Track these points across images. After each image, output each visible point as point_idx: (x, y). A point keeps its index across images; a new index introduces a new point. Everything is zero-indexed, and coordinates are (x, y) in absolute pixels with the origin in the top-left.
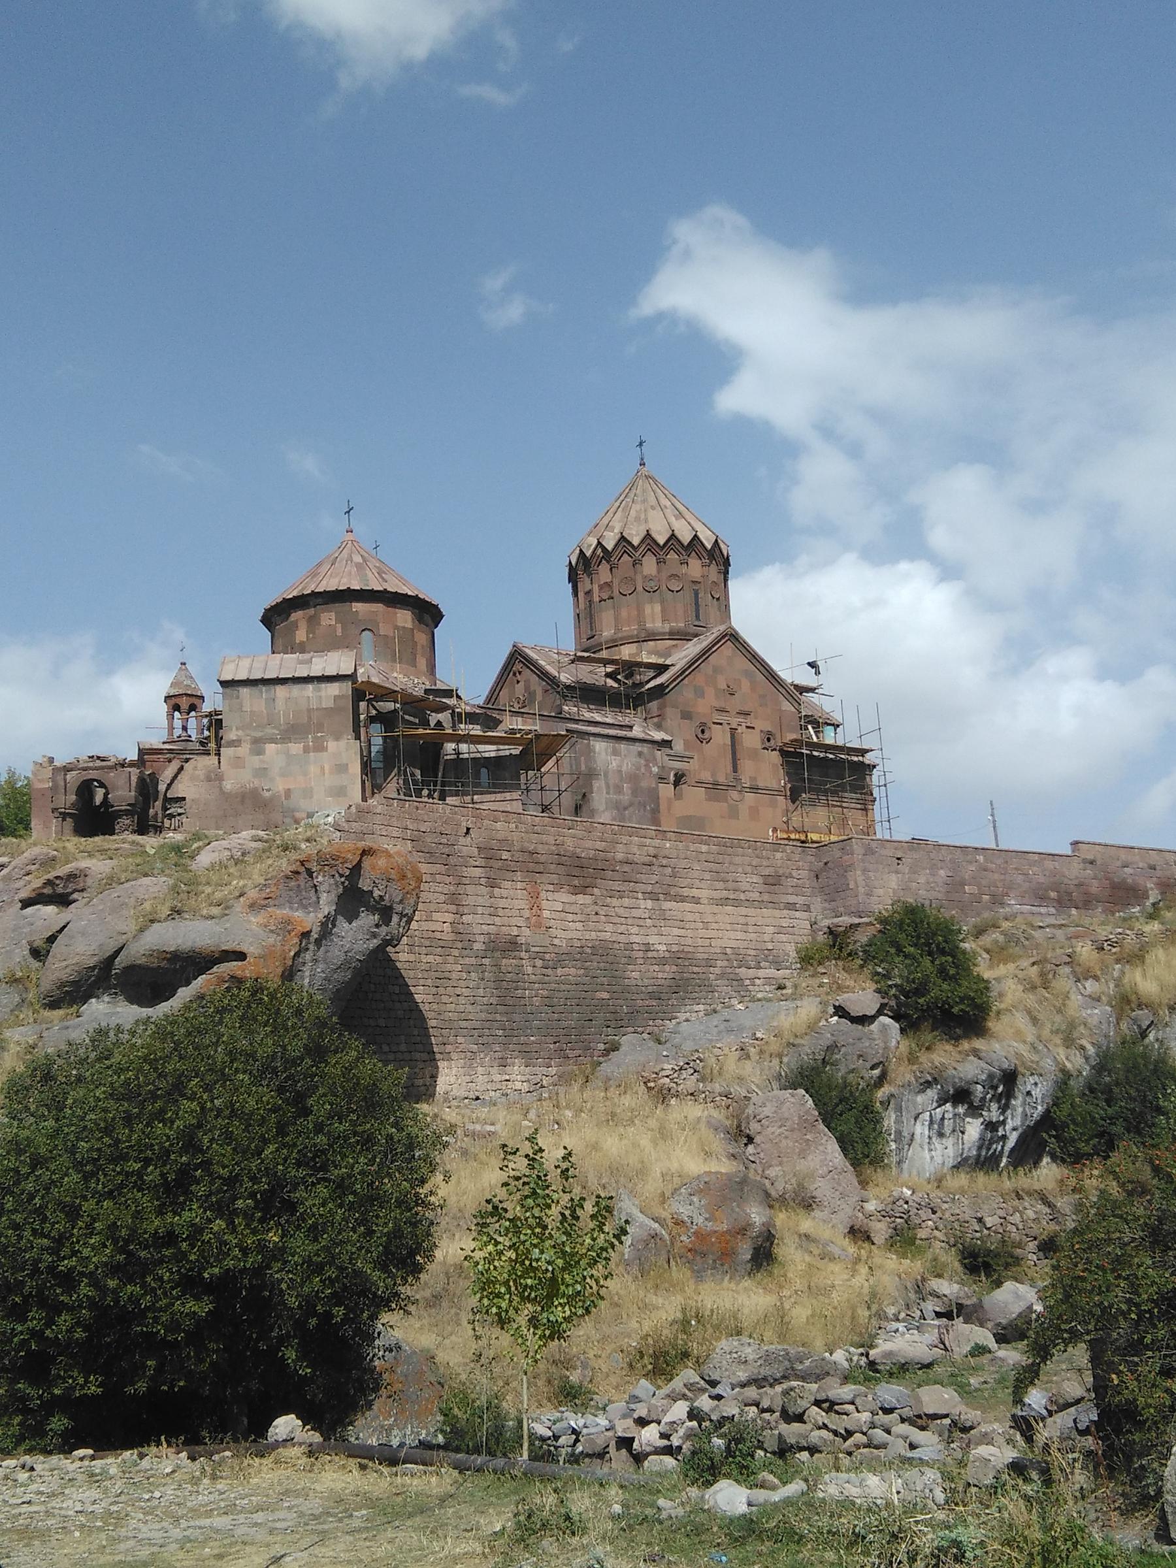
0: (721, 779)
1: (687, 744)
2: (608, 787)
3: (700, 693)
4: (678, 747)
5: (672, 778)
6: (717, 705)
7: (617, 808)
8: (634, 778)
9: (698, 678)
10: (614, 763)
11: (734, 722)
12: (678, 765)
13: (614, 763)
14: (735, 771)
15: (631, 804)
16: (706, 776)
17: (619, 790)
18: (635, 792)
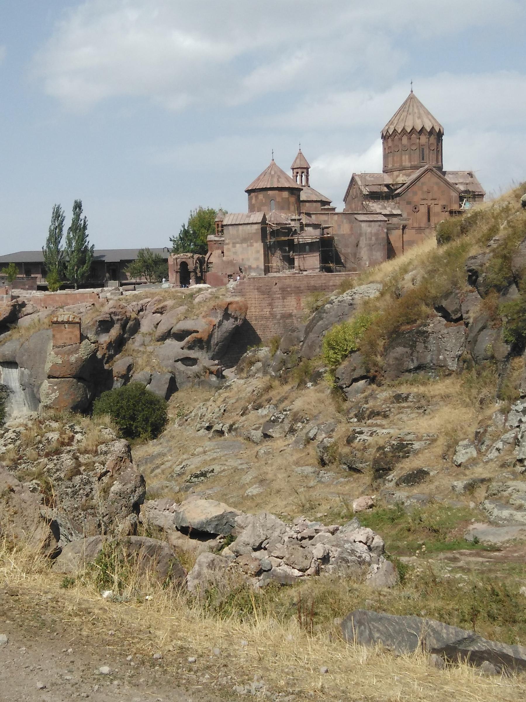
0: (423, 225)
1: (409, 214)
2: (366, 239)
3: (415, 193)
4: (405, 215)
5: (401, 227)
6: (422, 197)
7: (370, 246)
8: (377, 235)
9: (415, 188)
10: (369, 230)
11: (429, 202)
12: (404, 222)
13: (369, 230)
14: (429, 220)
15: (375, 244)
16: (416, 225)
17: (370, 239)
18: (377, 239)
